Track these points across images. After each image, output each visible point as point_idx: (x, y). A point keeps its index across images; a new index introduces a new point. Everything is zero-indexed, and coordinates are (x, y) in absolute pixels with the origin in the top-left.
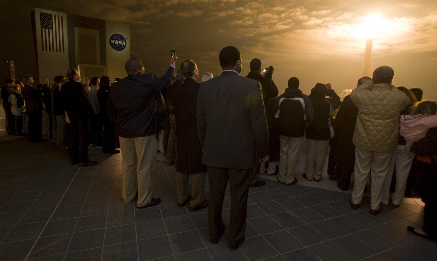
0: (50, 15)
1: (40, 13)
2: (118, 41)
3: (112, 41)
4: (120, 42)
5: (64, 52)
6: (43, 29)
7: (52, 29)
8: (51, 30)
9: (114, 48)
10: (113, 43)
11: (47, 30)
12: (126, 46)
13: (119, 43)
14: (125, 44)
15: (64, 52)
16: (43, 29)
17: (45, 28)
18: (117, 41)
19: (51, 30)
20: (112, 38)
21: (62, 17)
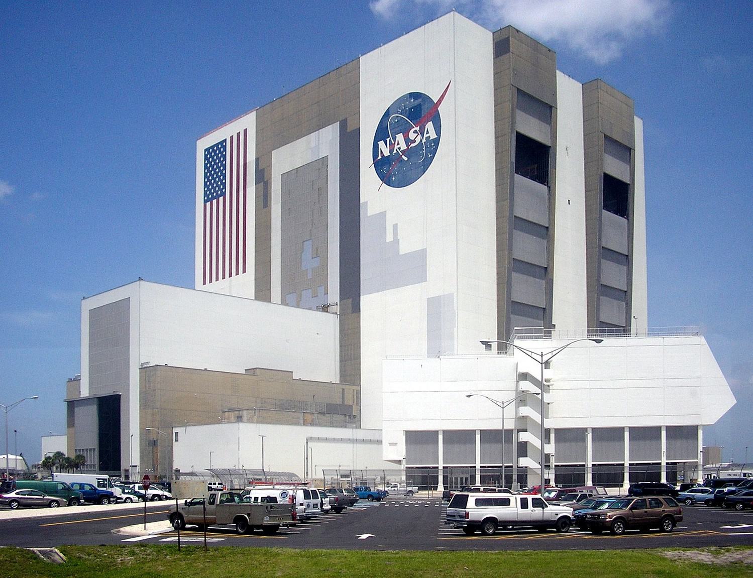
1: (205, 150)
3: (381, 144)
4: (412, 136)
6: (208, 204)
7: (224, 194)
8: (221, 199)
9: (386, 179)
10: (386, 153)
11: (215, 201)
12: (437, 142)
13: (408, 141)
14: (433, 135)
16: (208, 204)
17: (213, 198)
18: (400, 137)
19: (221, 199)
21: (245, 131)
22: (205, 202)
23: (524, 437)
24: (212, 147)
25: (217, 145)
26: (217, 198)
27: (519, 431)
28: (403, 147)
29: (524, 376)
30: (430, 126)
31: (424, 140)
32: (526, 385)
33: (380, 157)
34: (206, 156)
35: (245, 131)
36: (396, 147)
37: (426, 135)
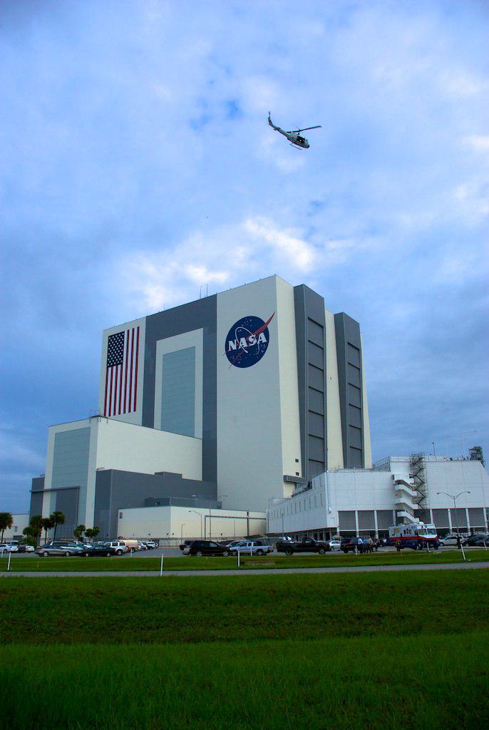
0: (121, 333)
2: (246, 336)
4: (250, 339)
5: (135, 410)
6: (110, 369)
7: (122, 364)
8: (119, 366)
10: (234, 348)
11: (115, 367)
12: (267, 344)
13: (248, 342)
14: (264, 340)
15: (135, 410)
16: (110, 369)
17: (113, 365)
18: (243, 340)
19: (119, 366)
20: (230, 337)
21: (138, 328)
22: (108, 367)
23: (403, 514)
24: (114, 335)
25: (118, 334)
26: (117, 365)
27: (397, 511)
28: (245, 345)
29: (399, 482)
30: (262, 335)
31: (259, 343)
32: (402, 487)
33: (230, 350)
34: (109, 340)
35: (138, 328)
36: (241, 345)
37: (259, 340)
